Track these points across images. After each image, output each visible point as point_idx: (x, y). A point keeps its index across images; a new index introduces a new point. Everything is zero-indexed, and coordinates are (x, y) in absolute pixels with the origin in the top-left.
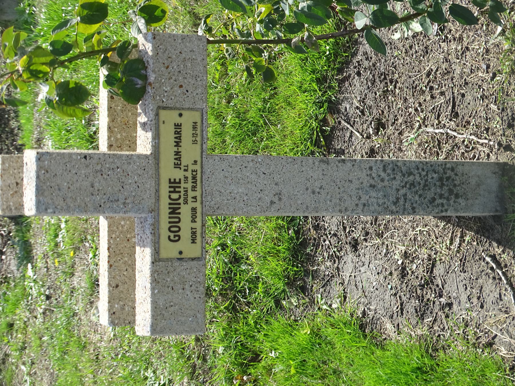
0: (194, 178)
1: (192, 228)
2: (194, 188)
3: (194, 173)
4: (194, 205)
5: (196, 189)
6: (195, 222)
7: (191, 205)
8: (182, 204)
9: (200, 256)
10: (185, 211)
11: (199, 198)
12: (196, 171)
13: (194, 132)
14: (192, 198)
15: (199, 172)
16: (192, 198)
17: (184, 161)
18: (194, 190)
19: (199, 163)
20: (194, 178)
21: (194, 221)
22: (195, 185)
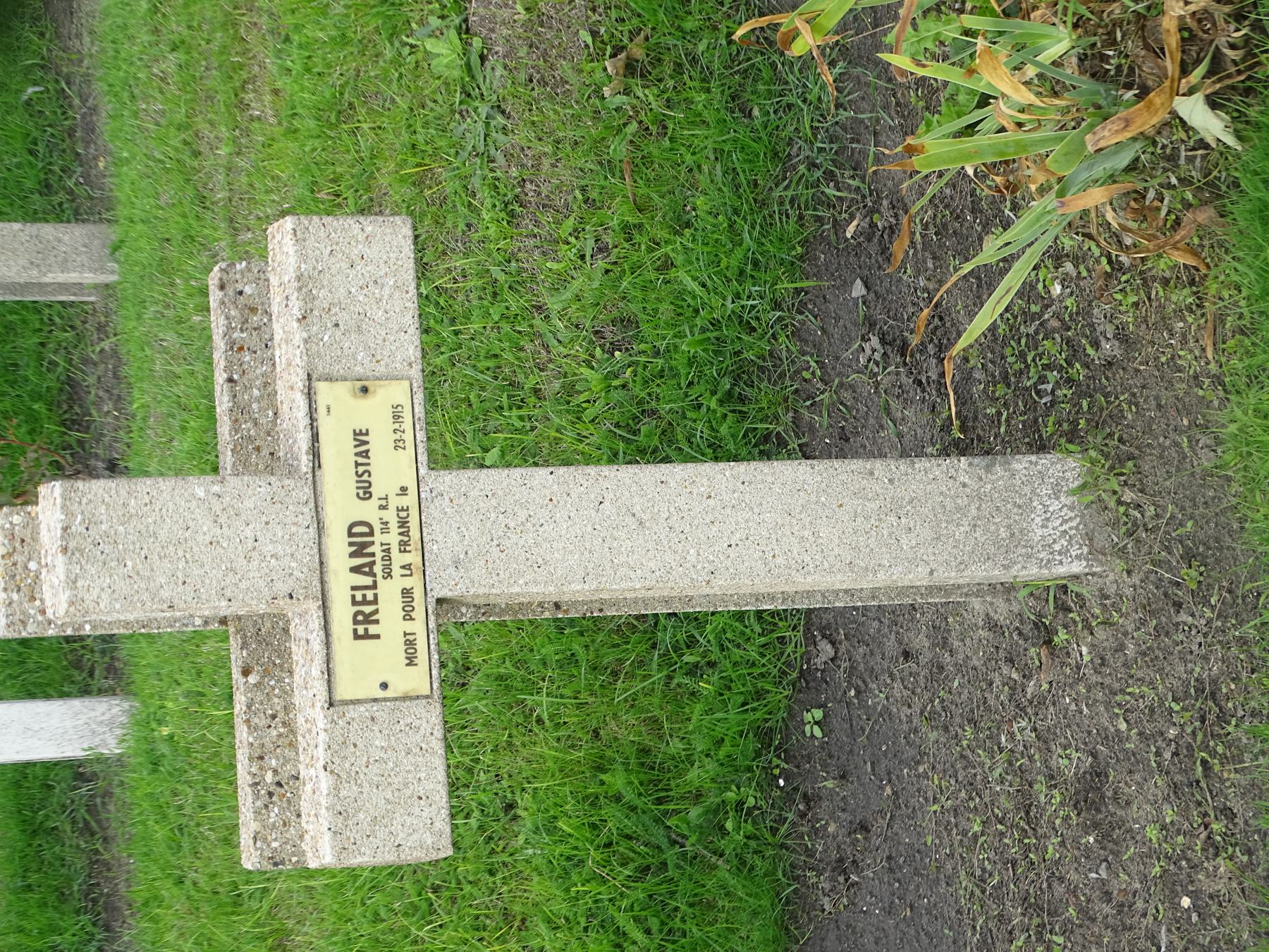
0: (403, 523)
1: (405, 634)
2: (404, 546)
3: (403, 514)
4: (408, 583)
5: (408, 548)
6: (412, 619)
9: (428, 693)
12: (408, 509)
13: (397, 426)
14: (403, 567)
16: (403, 567)
17: (377, 491)
18: (405, 551)
20: (403, 523)
21: (408, 617)
22: (406, 539)
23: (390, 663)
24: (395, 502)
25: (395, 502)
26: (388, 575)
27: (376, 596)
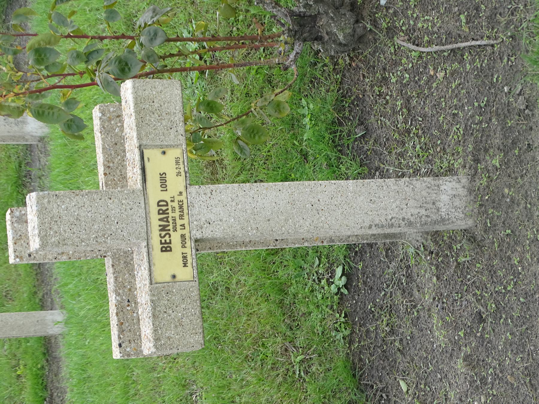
0: (181, 207)
2: (181, 217)
3: (181, 203)
4: (183, 232)
7: (180, 232)
8: (171, 232)
10: (176, 238)
11: (187, 226)
14: (181, 225)
15: (185, 201)
16: (181, 225)
18: (182, 219)
19: (184, 194)
20: (181, 207)
21: (184, 246)
22: (182, 214)
23: (175, 267)
24: (177, 198)
25: (177, 198)
26: (175, 230)
27: (170, 240)
